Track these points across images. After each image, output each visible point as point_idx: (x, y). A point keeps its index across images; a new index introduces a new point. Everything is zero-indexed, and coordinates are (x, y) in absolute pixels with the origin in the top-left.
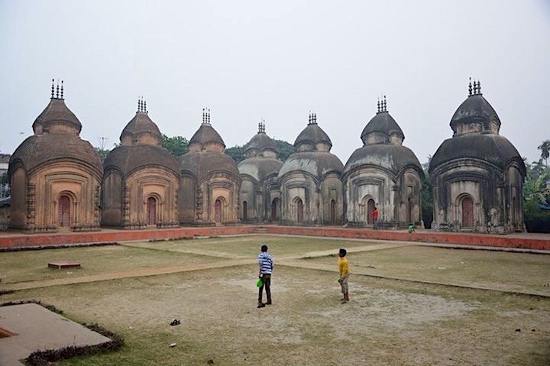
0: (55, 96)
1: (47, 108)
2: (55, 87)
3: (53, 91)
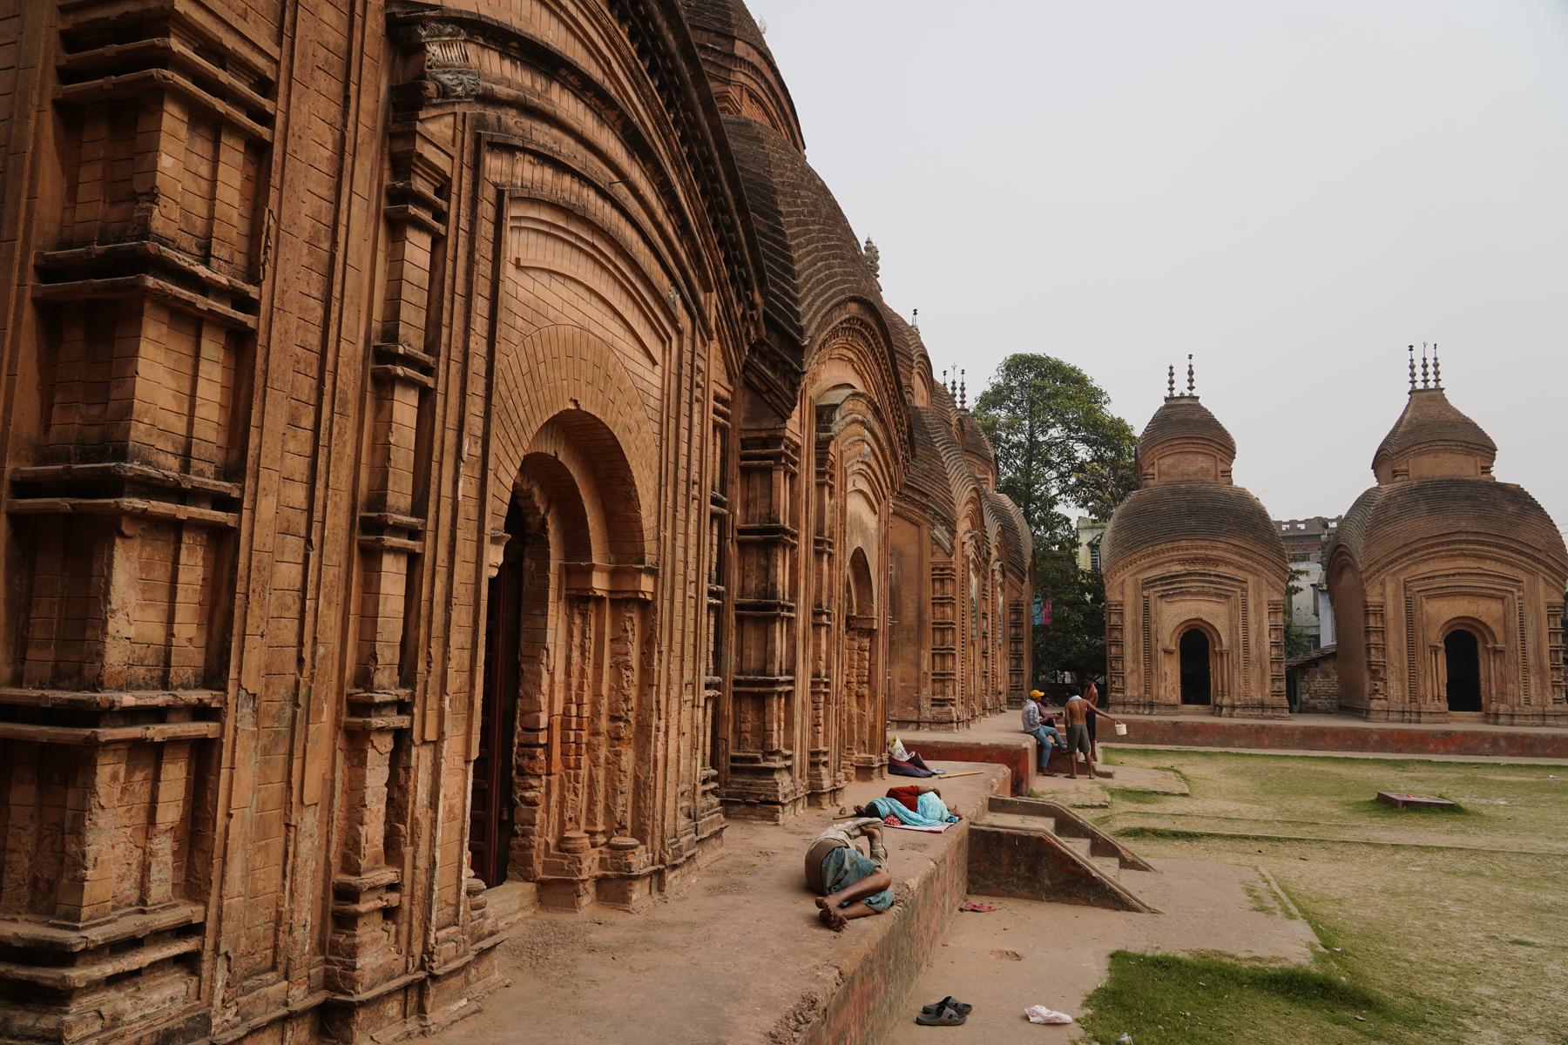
0: (1420, 385)
1: (1402, 418)
2: (1418, 363)
3: (1413, 375)
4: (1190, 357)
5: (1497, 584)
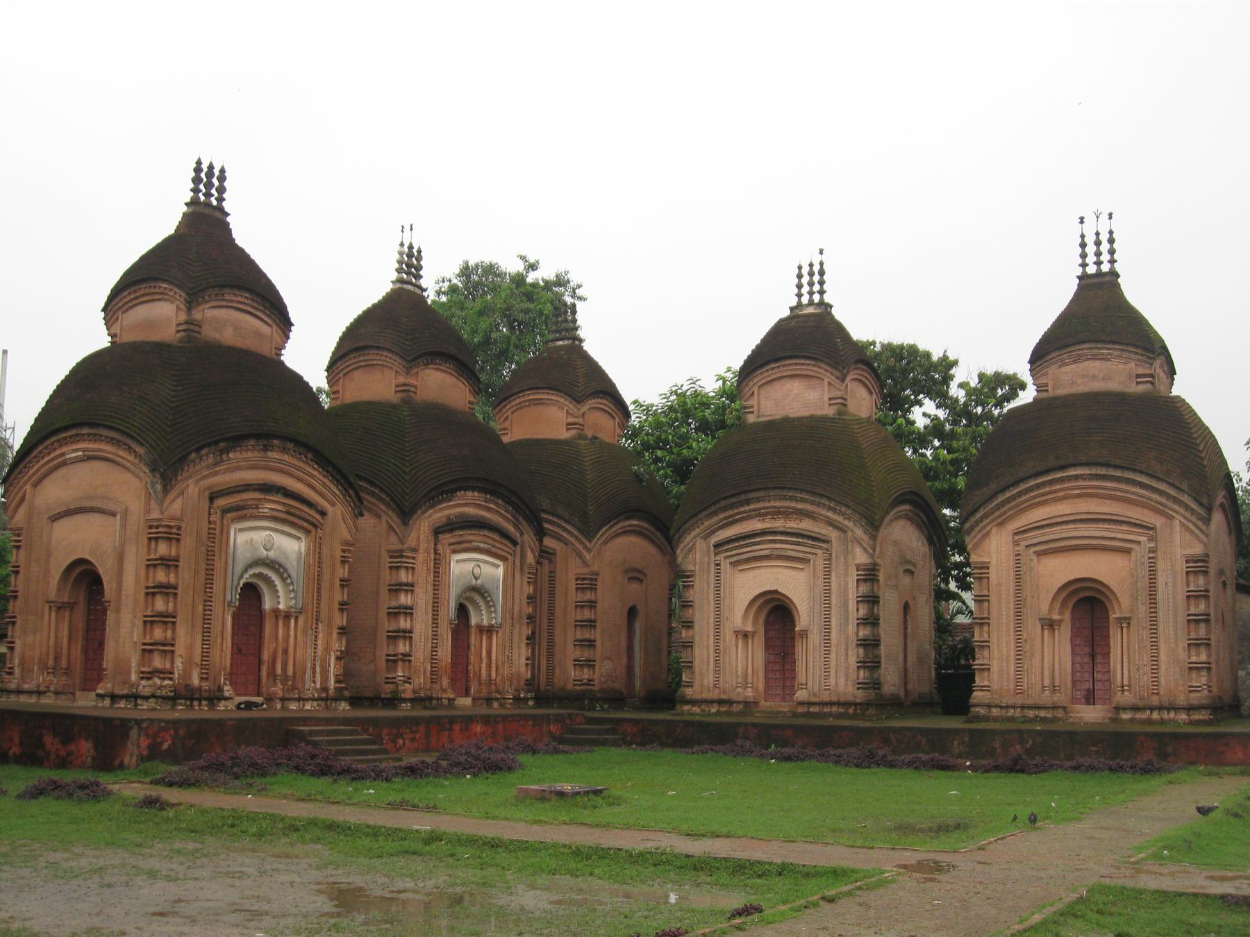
0: (1091, 269)
2: (1090, 240)
3: (1084, 256)
4: (821, 252)
5: (1123, 533)
